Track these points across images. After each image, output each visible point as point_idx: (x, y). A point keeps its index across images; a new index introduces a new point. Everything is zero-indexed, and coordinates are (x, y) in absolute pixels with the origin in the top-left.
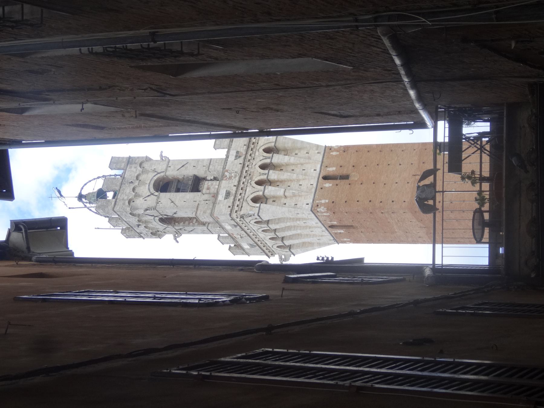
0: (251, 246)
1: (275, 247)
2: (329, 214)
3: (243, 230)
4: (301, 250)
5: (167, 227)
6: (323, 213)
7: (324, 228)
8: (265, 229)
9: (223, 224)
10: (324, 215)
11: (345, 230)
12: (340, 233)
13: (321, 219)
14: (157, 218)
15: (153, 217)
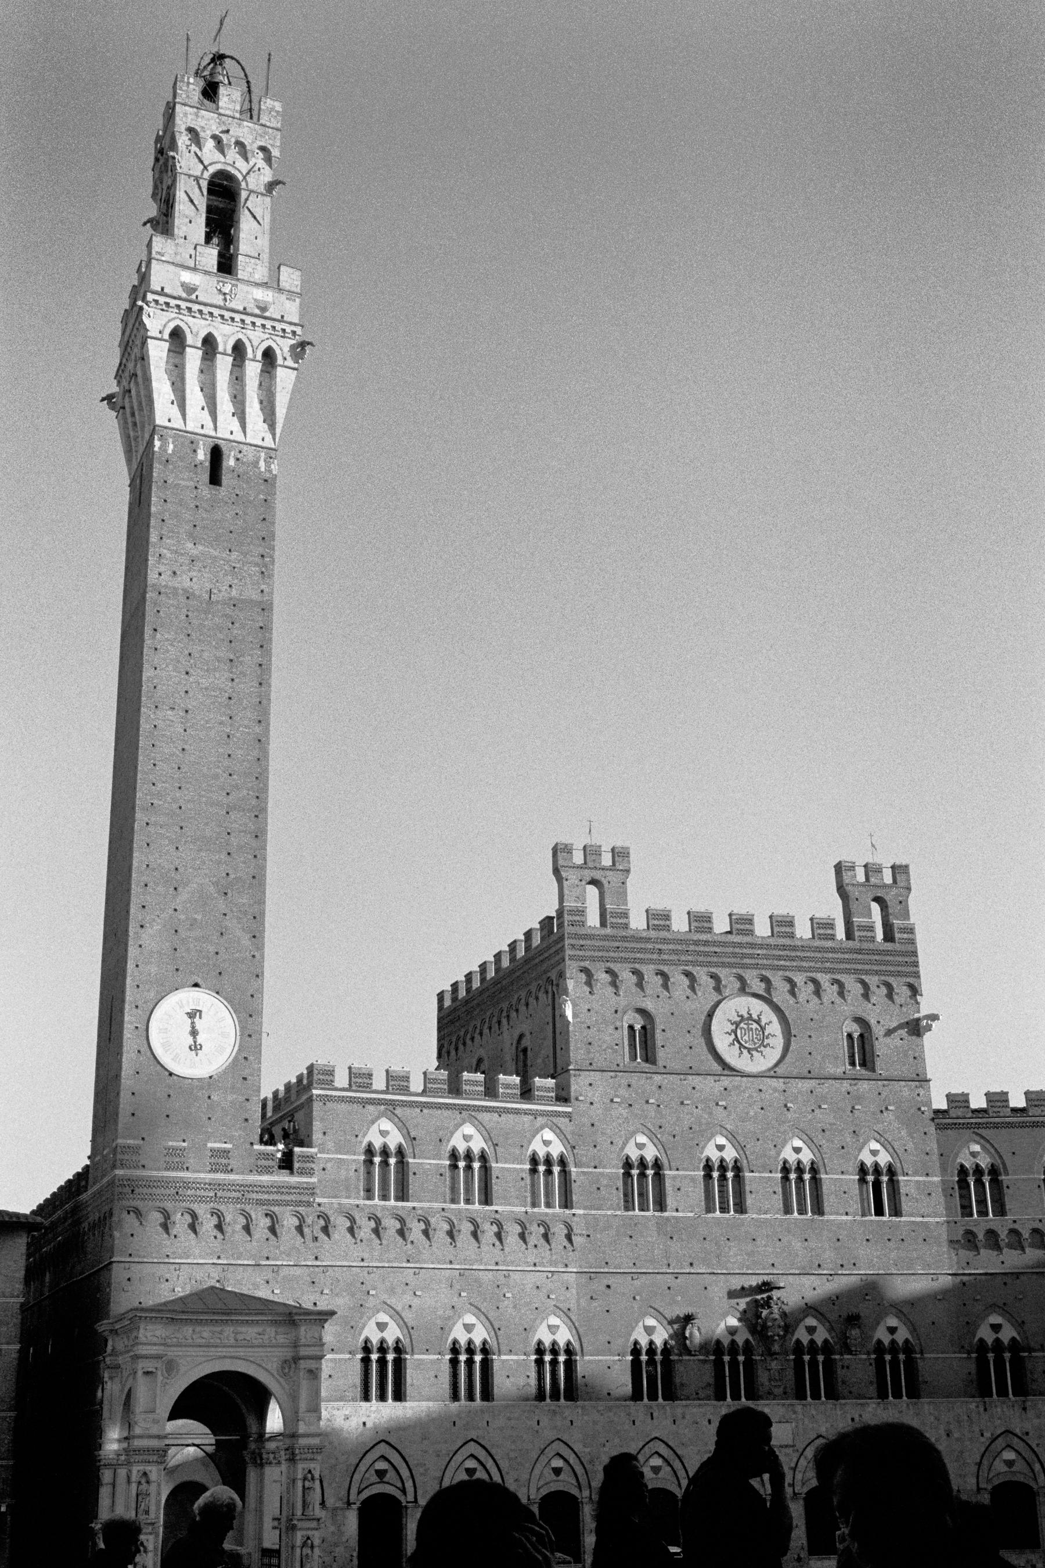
0: (190, 289)
1: (177, 322)
2: (263, 469)
3: (244, 312)
4: (161, 358)
5: (205, 168)
6: (265, 461)
7: (213, 433)
8: (249, 350)
9: (270, 293)
10: (259, 458)
11: (207, 464)
12: (195, 451)
13: (245, 448)
14: (240, 177)
15: (244, 174)
